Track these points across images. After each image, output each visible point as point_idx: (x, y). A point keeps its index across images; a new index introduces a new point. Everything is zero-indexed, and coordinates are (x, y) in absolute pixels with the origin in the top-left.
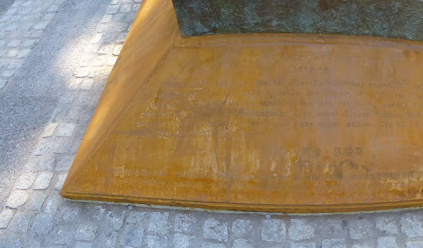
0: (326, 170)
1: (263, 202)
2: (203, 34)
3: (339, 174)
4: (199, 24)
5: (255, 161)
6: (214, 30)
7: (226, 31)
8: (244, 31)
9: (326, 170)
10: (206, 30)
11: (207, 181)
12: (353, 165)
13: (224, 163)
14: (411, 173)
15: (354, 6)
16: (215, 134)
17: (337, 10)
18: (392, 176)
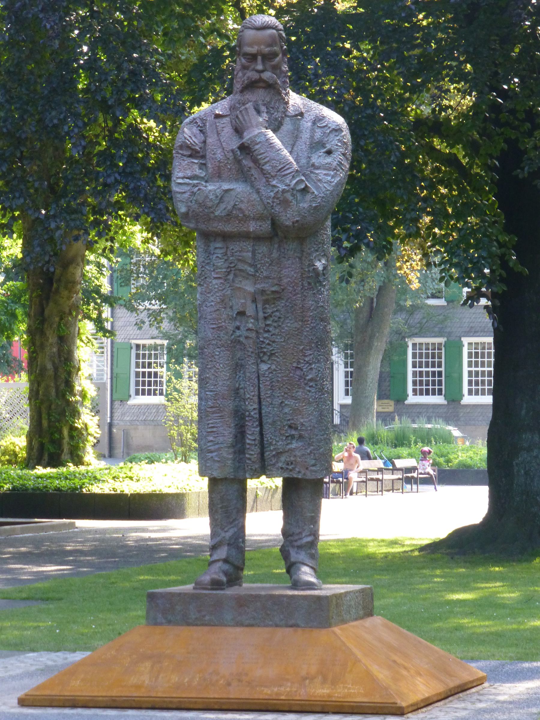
0: (221, 682)
1: (174, 695)
2: (161, 624)
3: (229, 684)
4: (160, 616)
5: (175, 678)
6: (169, 622)
7: (176, 623)
8: (188, 624)
9: (221, 682)
10: (164, 621)
11: (138, 687)
12: (240, 681)
13: (154, 679)
14: (281, 686)
15: (258, 604)
16: (152, 667)
17: (248, 607)
18: (266, 687)
